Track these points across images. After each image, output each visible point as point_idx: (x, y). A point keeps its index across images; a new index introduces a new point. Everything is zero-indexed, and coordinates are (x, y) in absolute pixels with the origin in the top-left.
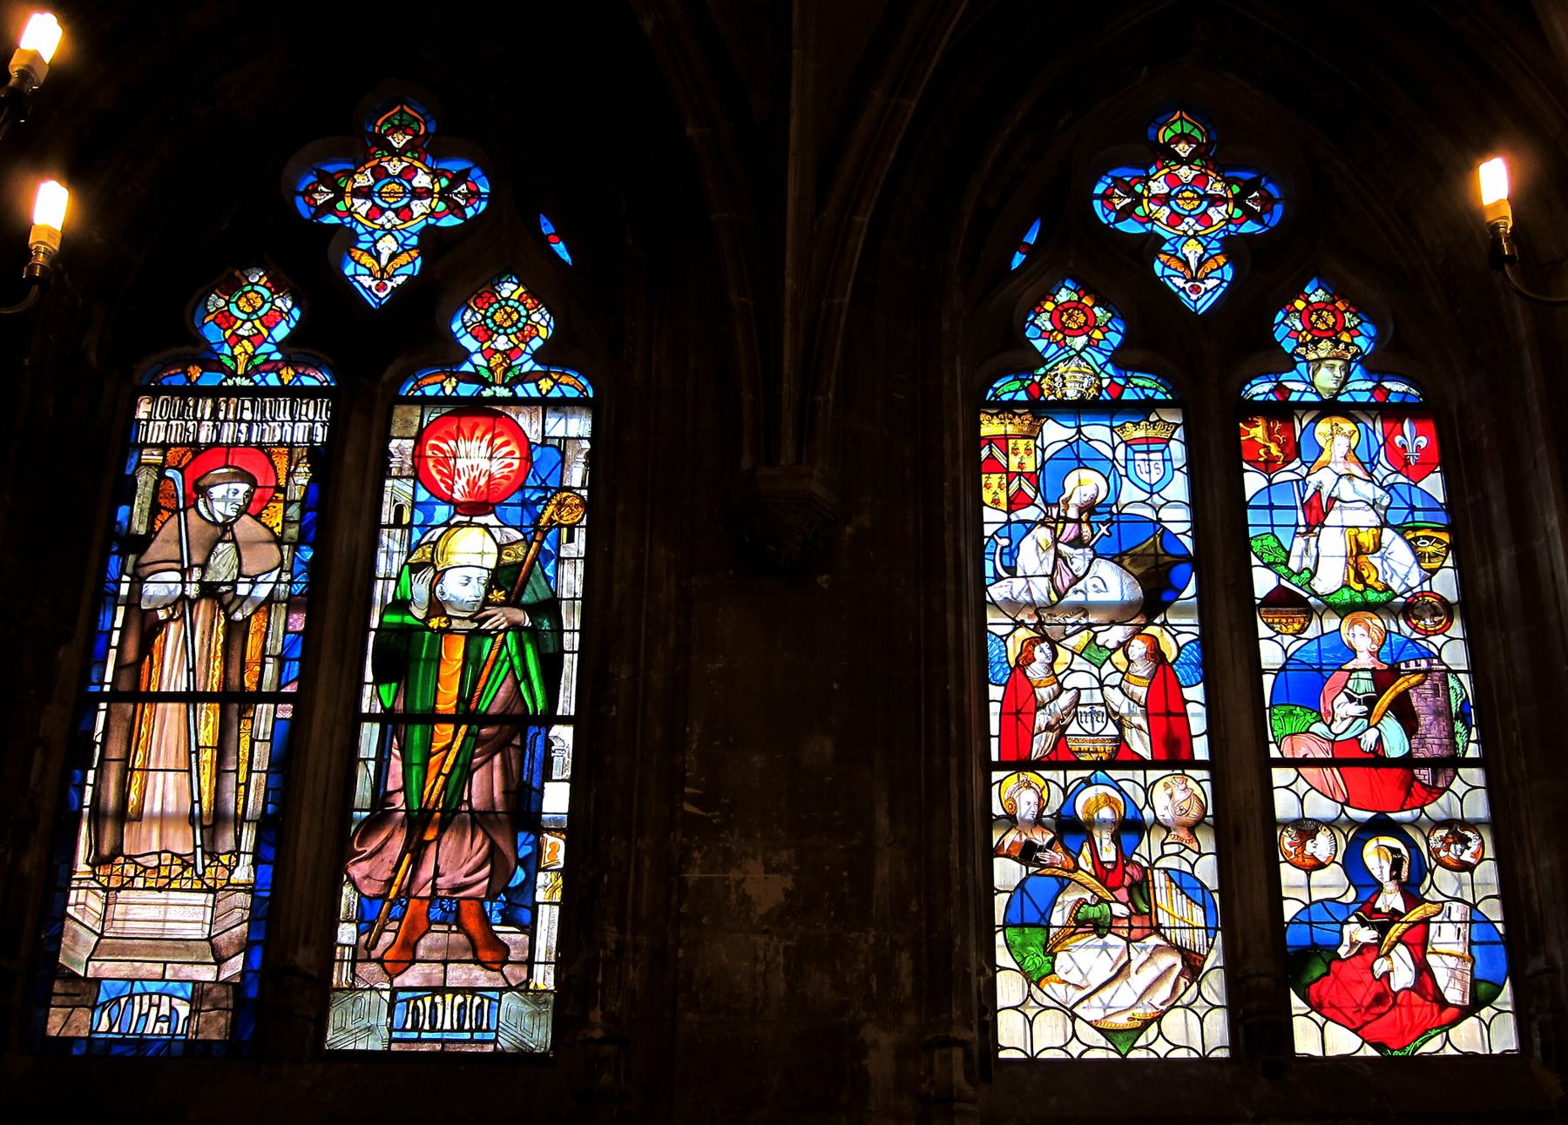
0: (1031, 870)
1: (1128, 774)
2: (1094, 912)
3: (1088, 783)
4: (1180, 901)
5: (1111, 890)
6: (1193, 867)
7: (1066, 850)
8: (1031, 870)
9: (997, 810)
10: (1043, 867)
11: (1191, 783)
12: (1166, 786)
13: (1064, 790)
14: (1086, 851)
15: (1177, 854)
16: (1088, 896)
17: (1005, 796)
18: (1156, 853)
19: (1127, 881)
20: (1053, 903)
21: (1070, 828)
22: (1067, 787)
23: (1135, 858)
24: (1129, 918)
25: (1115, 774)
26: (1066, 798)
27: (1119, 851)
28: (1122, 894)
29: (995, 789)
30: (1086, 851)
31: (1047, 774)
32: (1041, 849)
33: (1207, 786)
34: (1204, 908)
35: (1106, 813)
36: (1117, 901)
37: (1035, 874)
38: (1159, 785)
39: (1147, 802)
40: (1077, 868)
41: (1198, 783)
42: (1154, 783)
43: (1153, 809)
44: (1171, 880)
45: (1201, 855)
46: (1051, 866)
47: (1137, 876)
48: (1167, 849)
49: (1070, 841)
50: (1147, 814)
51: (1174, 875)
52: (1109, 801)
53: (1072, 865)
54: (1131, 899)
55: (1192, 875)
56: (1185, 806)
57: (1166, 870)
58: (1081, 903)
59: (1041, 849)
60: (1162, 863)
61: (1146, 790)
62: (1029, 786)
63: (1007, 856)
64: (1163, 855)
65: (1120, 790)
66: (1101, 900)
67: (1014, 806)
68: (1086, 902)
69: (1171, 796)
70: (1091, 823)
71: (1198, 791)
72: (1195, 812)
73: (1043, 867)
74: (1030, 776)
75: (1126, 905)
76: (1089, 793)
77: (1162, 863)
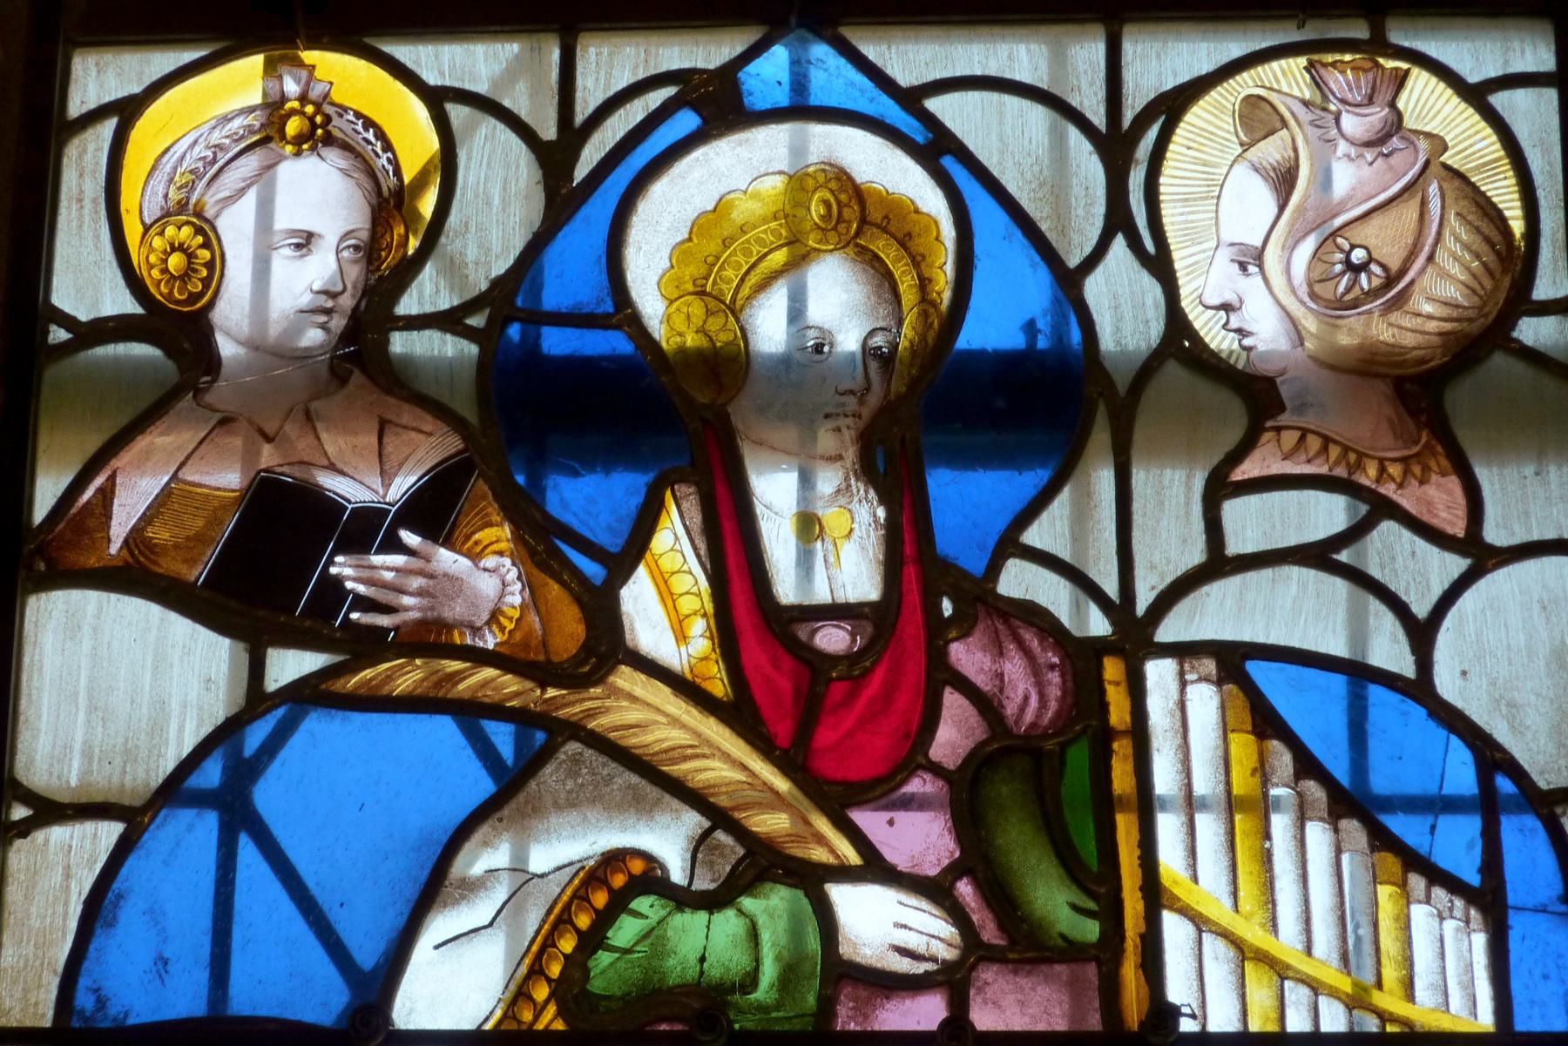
0: (289, 665)
1: (1020, 55)
2: (706, 942)
3: (718, 105)
4: (1314, 860)
5: (837, 798)
6: (1422, 634)
7: (542, 543)
8: (289, 665)
9: (84, 281)
10: (367, 646)
11: (1427, 103)
12: (1258, 118)
13: (554, 159)
14: (675, 541)
15: (1317, 555)
16: (668, 840)
17: (141, 196)
18: (1169, 541)
19: (954, 733)
20: (434, 889)
21: (587, 408)
22: (574, 134)
23: (1019, 581)
24: (953, 980)
25: (910, 57)
26: (561, 198)
27: (908, 543)
28: (919, 835)
29: (81, 166)
30: (675, 541)
31: (440, 60)
32: (366, 530)
33: (1534, 114)
34: (1489, 900)
35: (837, 306)
36: (875, 869)
37: (307, 694)
38: (1209, 120)
39: (1117, 219)
40: (607, 646)
41: (1476, 95)
42: (1173, 105)
43: (1160, 265)
44: (1266, 722)
45: (1483, 558)
46: (429, 639)
47: (1026, 689)
48: (1250, 523)
49: (589, 499)
50: (1122, 310)
51: (1314, 709)
52: (858, 221)
53: (570, 629)
54: (978, 856)
55: (1420, 688)
56: (1385, 240)
57: (1231, 662)
58: (620, 880)
59: (366, 530)
60: (1214, 615)
61: (1115, 146)
62: (321, 133)
63: (133, 575)
64: (1219, 564)
65: (938, 150)
66: (764, 864)
67: (209, 270)
68: (651, 880)
69: (1284, 181)
70: (726, 366)
71: (1469, 140)
72: (1444, 289)
73: (367, 646)
74: (343, 75)
75: (935, 890)
76: (738, 170)
77: (1214, 615)
